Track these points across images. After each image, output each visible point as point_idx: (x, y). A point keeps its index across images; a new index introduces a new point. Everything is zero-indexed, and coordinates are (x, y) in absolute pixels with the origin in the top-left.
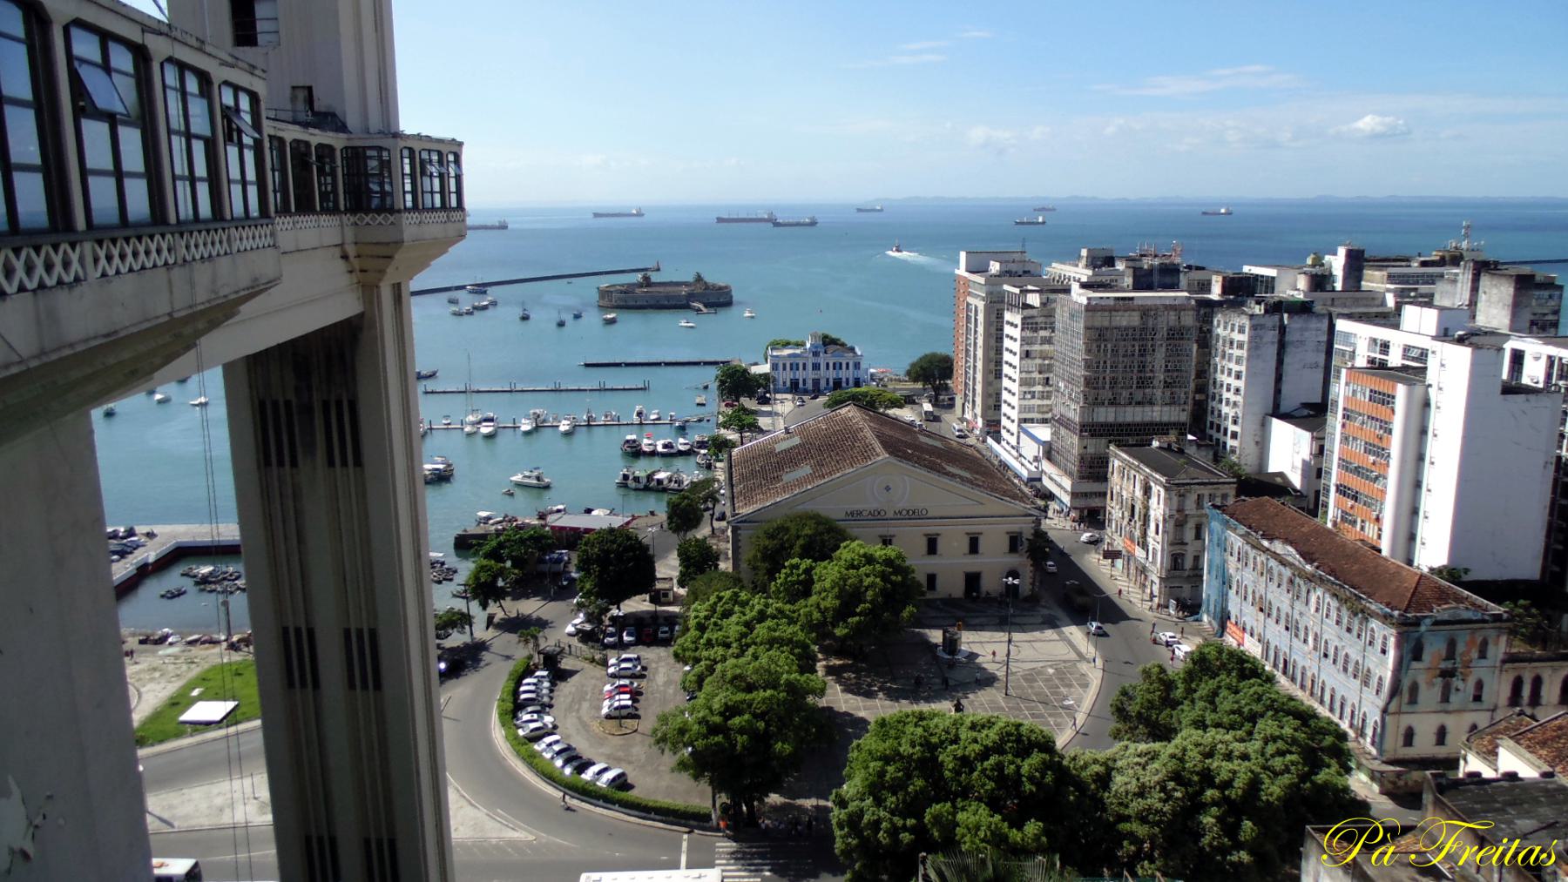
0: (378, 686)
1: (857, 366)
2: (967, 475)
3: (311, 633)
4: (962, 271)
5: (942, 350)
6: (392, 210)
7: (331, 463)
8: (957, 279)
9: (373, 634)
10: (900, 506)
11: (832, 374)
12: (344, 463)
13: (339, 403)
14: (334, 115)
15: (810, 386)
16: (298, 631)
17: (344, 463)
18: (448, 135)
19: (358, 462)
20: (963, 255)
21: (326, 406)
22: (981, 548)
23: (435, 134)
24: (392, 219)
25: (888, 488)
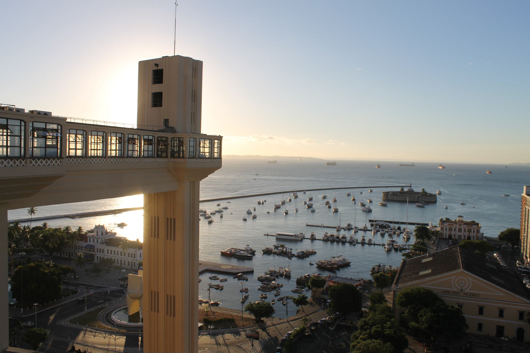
0: (174, 316)
1: (478, 231)
2: (502, 282)
3: (158, 293)
4: (524, 194)
5: (517, 227)
6: (183, 157)
7: (167, 238)
8: (523, 197)
9: (174, 297)
10: (467, 291)
11: (467, 234)
12: (171, 239)
13: (171, 219)
14: (173, 128)
15: (457, 237)
16: (155, 292)
17: (171, 239)
18: (218, 134)
19: (174, 239)
20: (525, 187)
21: (168, 219)
22: (504, 315)
23: (208, 134)
24: (184, 160)
25: (461, 283)
